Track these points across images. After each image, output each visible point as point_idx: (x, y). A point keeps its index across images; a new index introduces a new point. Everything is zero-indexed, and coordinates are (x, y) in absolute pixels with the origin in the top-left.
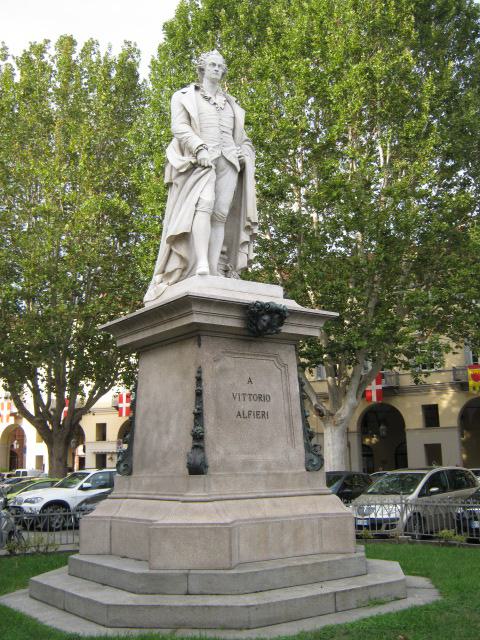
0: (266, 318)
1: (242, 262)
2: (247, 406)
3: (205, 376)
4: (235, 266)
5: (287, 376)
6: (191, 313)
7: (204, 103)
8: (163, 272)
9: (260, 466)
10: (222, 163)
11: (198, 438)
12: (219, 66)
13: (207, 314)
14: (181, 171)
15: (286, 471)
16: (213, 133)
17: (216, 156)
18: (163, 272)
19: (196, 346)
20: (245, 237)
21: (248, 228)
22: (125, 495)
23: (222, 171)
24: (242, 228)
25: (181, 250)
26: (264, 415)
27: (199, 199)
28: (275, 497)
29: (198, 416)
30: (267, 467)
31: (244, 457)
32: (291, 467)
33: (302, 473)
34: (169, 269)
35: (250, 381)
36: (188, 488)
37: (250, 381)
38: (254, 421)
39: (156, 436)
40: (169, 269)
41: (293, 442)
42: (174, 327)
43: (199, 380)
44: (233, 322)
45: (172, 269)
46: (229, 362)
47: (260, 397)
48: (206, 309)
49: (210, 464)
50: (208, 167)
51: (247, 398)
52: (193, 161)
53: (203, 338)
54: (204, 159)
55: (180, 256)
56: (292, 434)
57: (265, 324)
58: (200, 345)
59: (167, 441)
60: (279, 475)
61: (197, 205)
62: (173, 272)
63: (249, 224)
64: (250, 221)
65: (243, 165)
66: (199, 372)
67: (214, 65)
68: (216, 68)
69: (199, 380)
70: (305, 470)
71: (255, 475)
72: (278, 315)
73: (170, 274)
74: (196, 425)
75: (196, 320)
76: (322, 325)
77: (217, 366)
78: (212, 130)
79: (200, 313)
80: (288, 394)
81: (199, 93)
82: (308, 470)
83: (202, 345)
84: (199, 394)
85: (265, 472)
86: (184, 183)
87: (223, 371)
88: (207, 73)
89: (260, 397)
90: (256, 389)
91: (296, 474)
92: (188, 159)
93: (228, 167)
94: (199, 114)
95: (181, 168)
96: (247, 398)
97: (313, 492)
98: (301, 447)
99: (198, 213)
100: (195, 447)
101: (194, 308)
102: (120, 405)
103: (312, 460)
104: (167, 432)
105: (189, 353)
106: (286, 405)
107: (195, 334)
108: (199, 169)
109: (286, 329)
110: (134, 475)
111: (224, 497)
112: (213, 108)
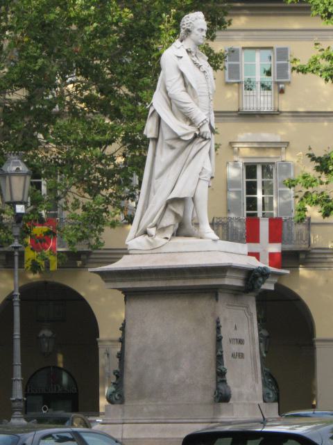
3: (222, 323)
6: (224, 277)
8: (156, 226)
9: (245, 397)
11: (221, 375)
14: (183, 138)
19: (214, 300)
22: (122, 421)
26: (241, 356)
27: (203, 168)
28: (195, 423)
29: (219, 358)
30: (247, 399)
36: (219, 412)
38: (239, 360)
39: (159, 370)
42: (211, 284)
44: (236, 281)
45: (168, 225)
50: (209, 139)
53: (219, 293)
54: (207, 132)
56: (256, 371)
58: (217, 300)
59: (175, 377)
61: (200, 174)
62: (167, 227)
66: (218, 322)
67: (202, 30)
69: (218, 328)
70: (262, 401)
71: (245, 404)
73: (163, 229)
79: (231, 277)
80: (253, 339)
82: (265, 401)
83: (219, 301)
85: (247, 402)
86: (183, 149)
88: (193, 36)
92: (192, 129)
95: (184, 135)
99: (201, 182)
101: (228, 274)
103: (269, 394)
105: (203, 305)
106: (252, 348)
107: (213, 292)
110: (126, 403)
112: (202, 75)
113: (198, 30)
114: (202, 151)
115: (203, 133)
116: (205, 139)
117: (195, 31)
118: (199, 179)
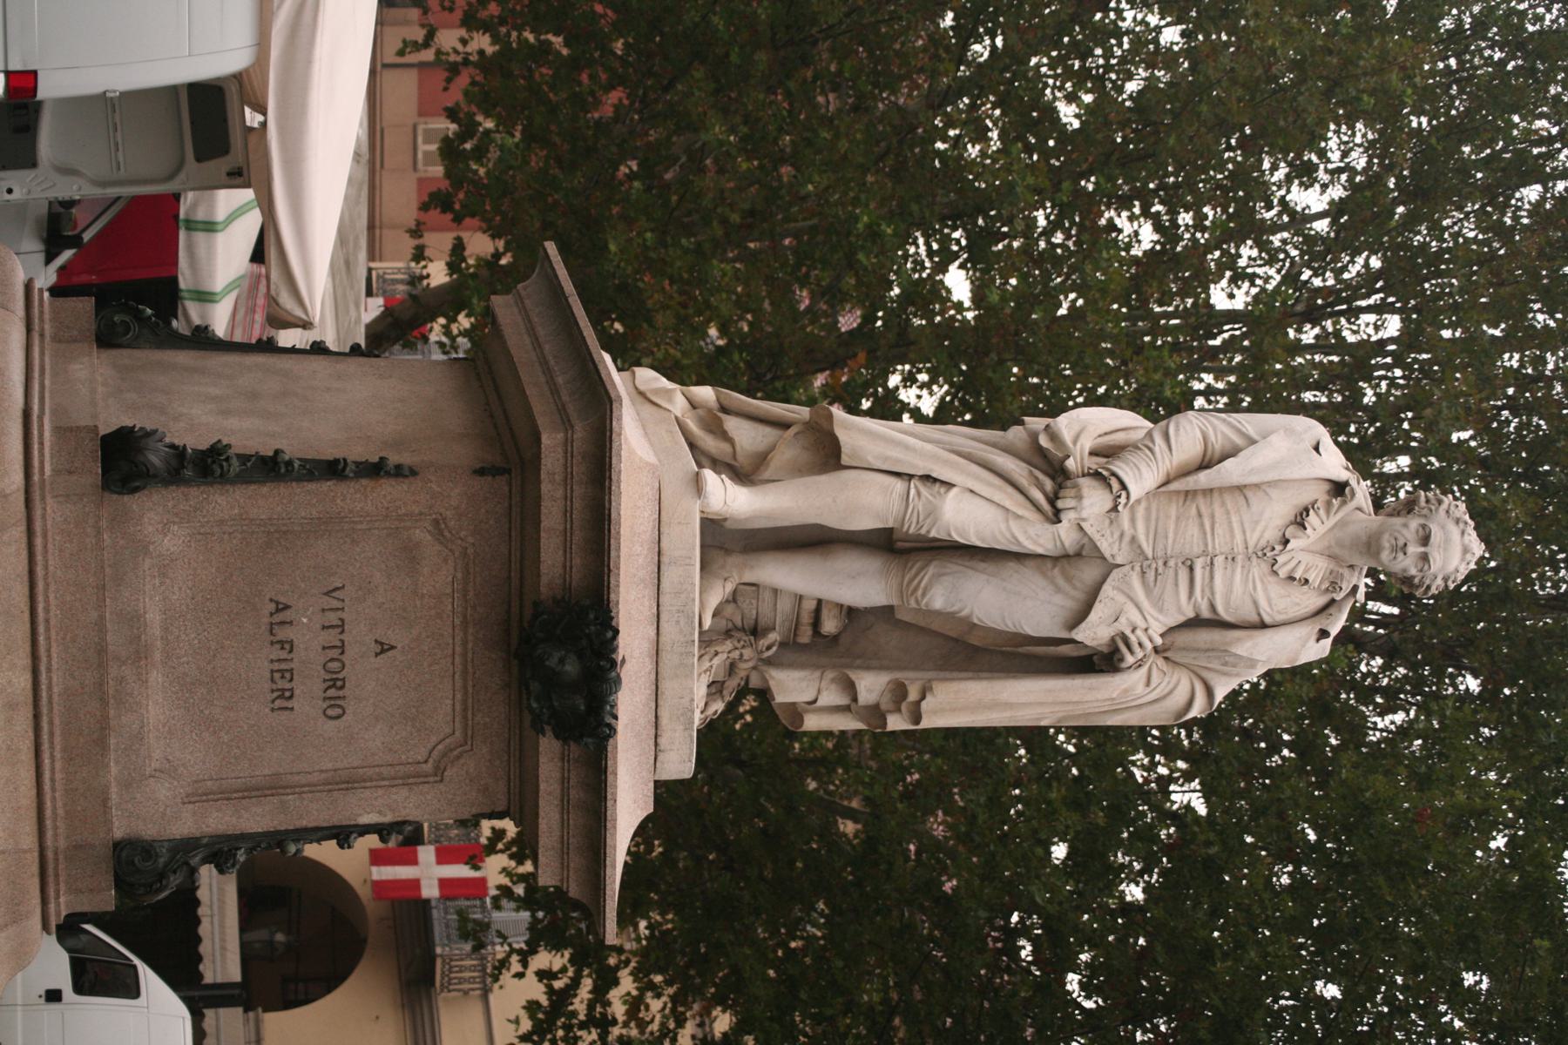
0: (571, 668)
1: (792, 686)
2: (307, 634)
3: (388, 491)
4: (769, 662)
5: (410, 779)
7: (1274, 513)
10: (1089, 573)
12: (1425, 558)
13: (567, 479)
15: (114, 769)
16: (1184, 535)
17: (1105, 546)
18: (724, 410)
20: (871, 686)
21: (899, 692)
23: (1069, 579)
24: (899, 675)
25: (789, 450)
26: (286, 695)
27: (949, 485)
31: (154, 617)
32: (126, 785)
33: (108, 823)
34: (732, 424)
35: (384, 648)
37: (384, 648)
40: (732, 424)
41: (200, 796)
43: (375, 470)
46: (438, 575)
47: (335, 683)
48: (579, 469)
49: (133, 502)
51: (331, 637)
52: (1071, 464)
53: (501, 481)
54: (1079, 497)
55: (772, 448)
57: (552, 662)
58: (481, 472)
60: (101, 743)
61: (928, 479)
62: (725, 436)
63: (913, 695)
64: (923, 698)
65: (1104, 661)
66: (399, 472)
67: (1425, 540)
68: (1415, 549)
70: (119, 833)
72: (586, 723)
74: (243, 458)
75: (546, 440)
76: (574, 891)
77: (422, 535)
78: (1193, 530)
81: (1319, 493)
84: (333, 469)
87: (410, 555)
89: (335, 683)
90: (363, 671)
91: (105, 801)
93: (1080, 595)
94: (1240, 489)
96: (331, 637)
97: (50, 855)
98: (185, 825)
99: (899, 485)
100: (179, 452)
102: (427, 853)
104: (226, 413)
106: (315, 778)
108: (1049, 485)
109: (548, 747)
111: (39, 541)
112: (1272, 535)
113: (1424, 526)
114: (1010, 489)
115: (1076, 486)
116: (1052, 500)
117: (1415, 523)
118: (911, 477)
